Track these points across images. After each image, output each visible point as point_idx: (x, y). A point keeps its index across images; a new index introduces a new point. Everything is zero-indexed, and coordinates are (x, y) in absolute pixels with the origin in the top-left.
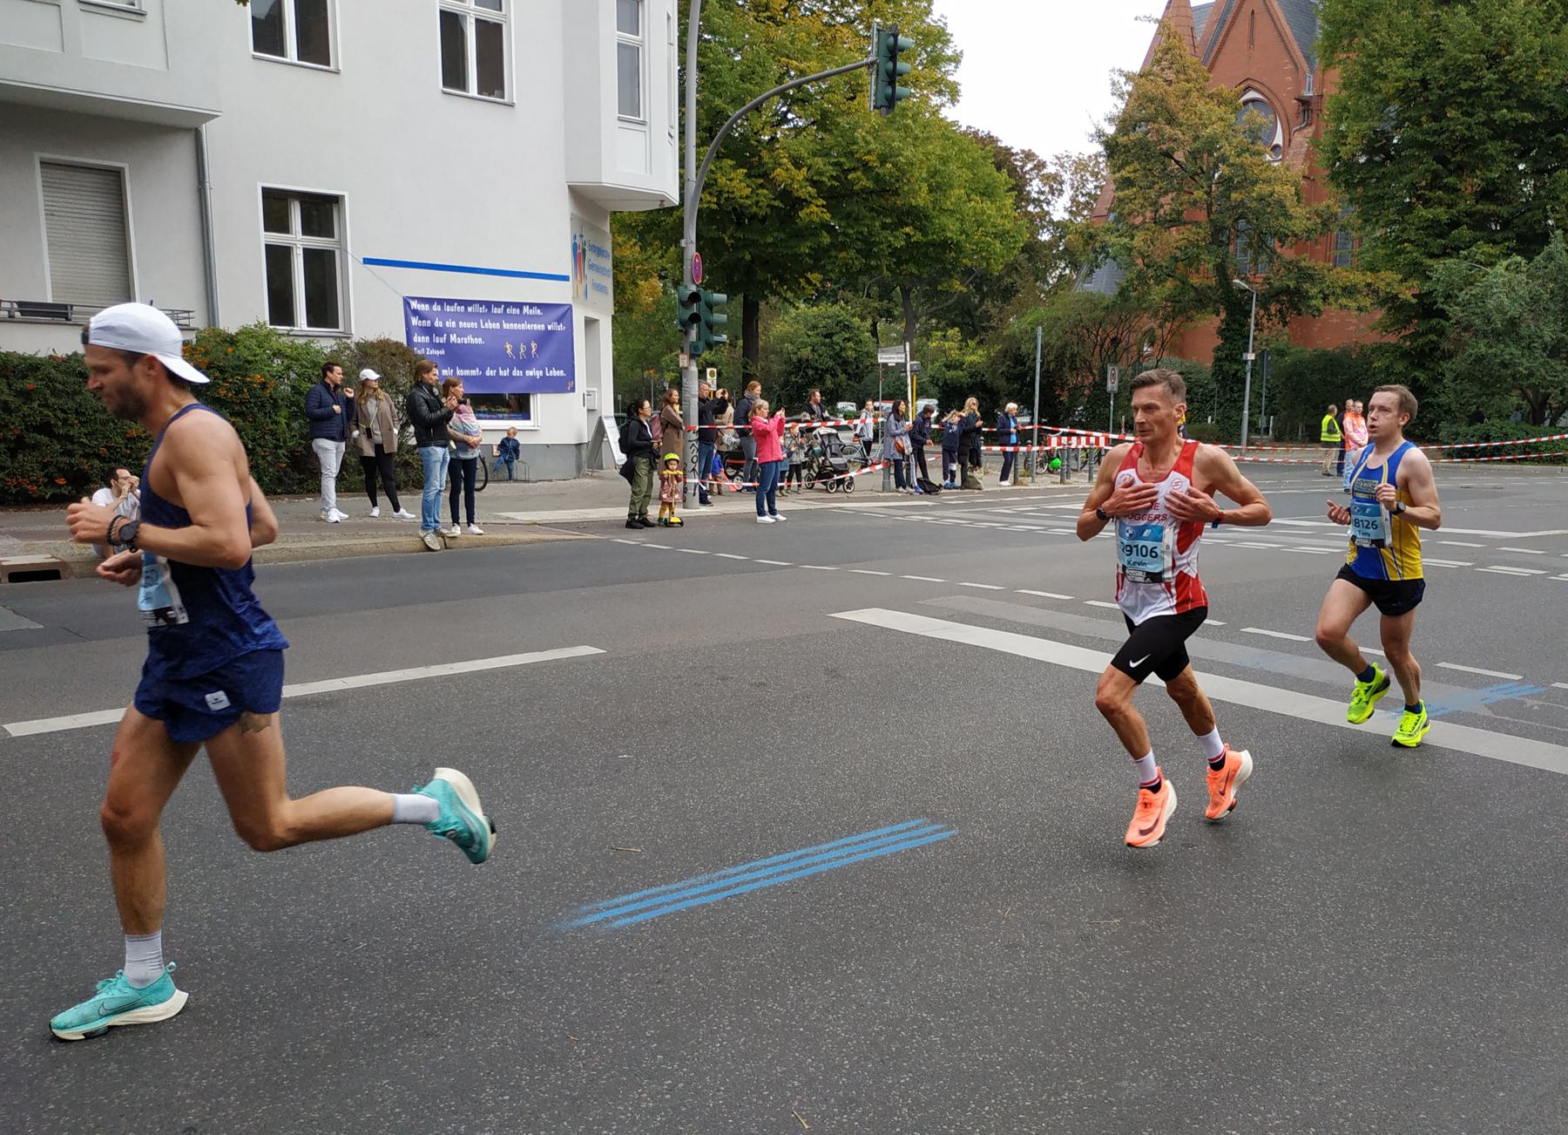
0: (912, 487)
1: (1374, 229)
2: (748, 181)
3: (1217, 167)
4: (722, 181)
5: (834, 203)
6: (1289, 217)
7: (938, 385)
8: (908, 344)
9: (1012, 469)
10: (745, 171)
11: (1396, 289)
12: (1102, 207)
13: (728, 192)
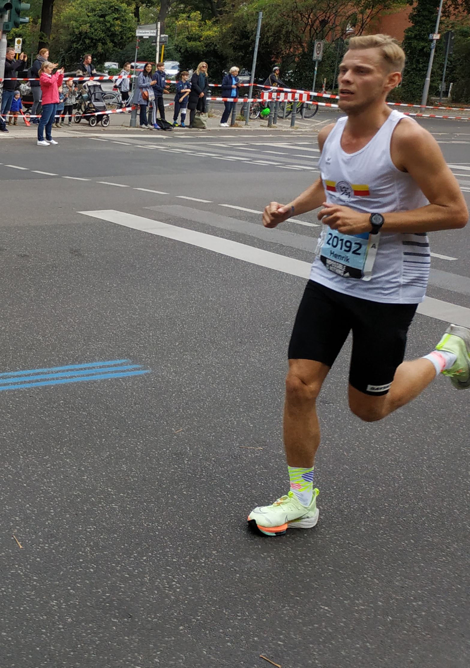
0: (152, 125)
7: (180, 51)
9: (231, 114)
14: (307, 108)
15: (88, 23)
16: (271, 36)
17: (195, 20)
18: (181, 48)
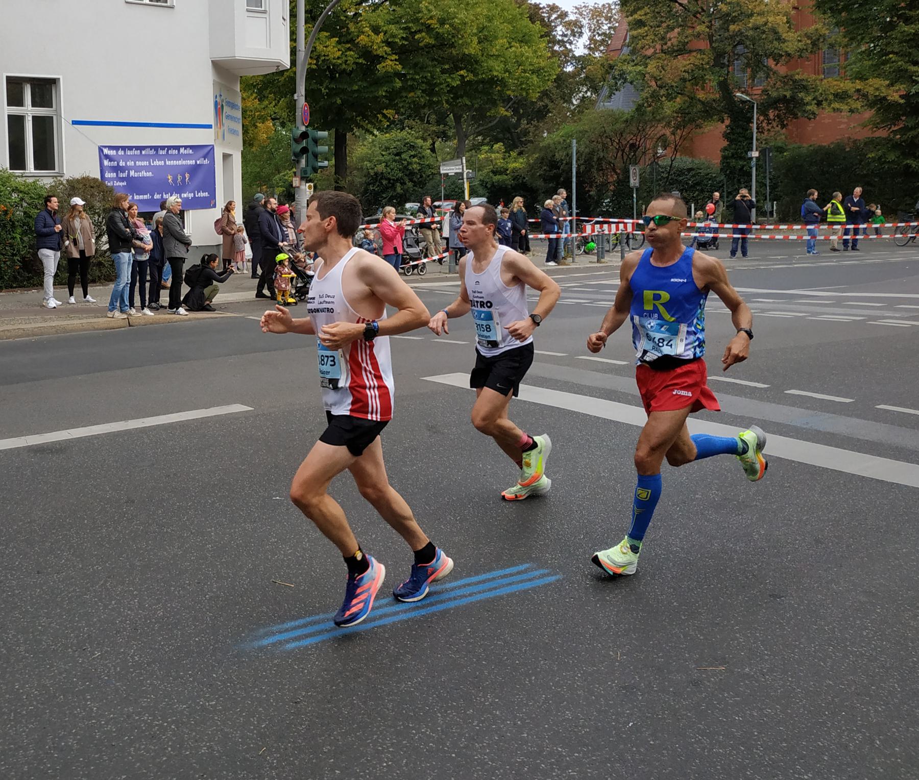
1: (859, 46)
2: (339, 47)
3: (716, 5)
4: (320, 48)
5: (404, 56)
6: (784, 41)
7: (486, 187)
8: (464, 158)
10: (337, 39)
11: (884, 92)
12: (618, 44)
13: (324, 56)
14: (633, 238)
15: (384, 162)
16: (583, 164)
17: (498, 152)
18: (486, 184)
